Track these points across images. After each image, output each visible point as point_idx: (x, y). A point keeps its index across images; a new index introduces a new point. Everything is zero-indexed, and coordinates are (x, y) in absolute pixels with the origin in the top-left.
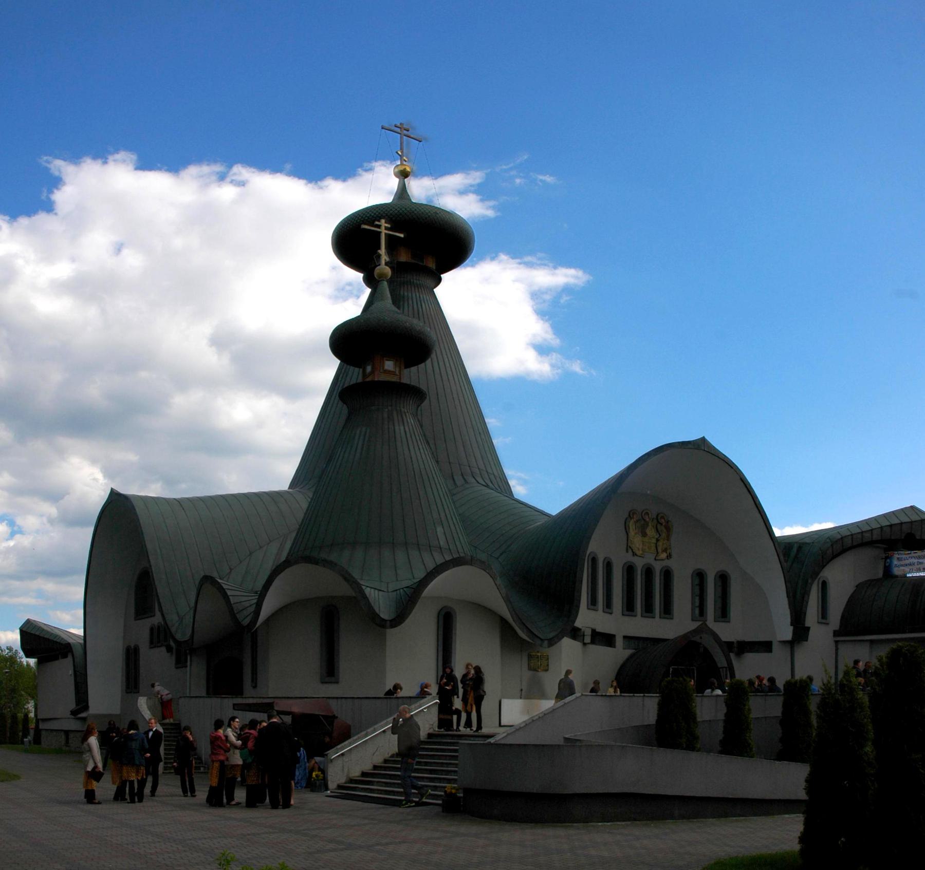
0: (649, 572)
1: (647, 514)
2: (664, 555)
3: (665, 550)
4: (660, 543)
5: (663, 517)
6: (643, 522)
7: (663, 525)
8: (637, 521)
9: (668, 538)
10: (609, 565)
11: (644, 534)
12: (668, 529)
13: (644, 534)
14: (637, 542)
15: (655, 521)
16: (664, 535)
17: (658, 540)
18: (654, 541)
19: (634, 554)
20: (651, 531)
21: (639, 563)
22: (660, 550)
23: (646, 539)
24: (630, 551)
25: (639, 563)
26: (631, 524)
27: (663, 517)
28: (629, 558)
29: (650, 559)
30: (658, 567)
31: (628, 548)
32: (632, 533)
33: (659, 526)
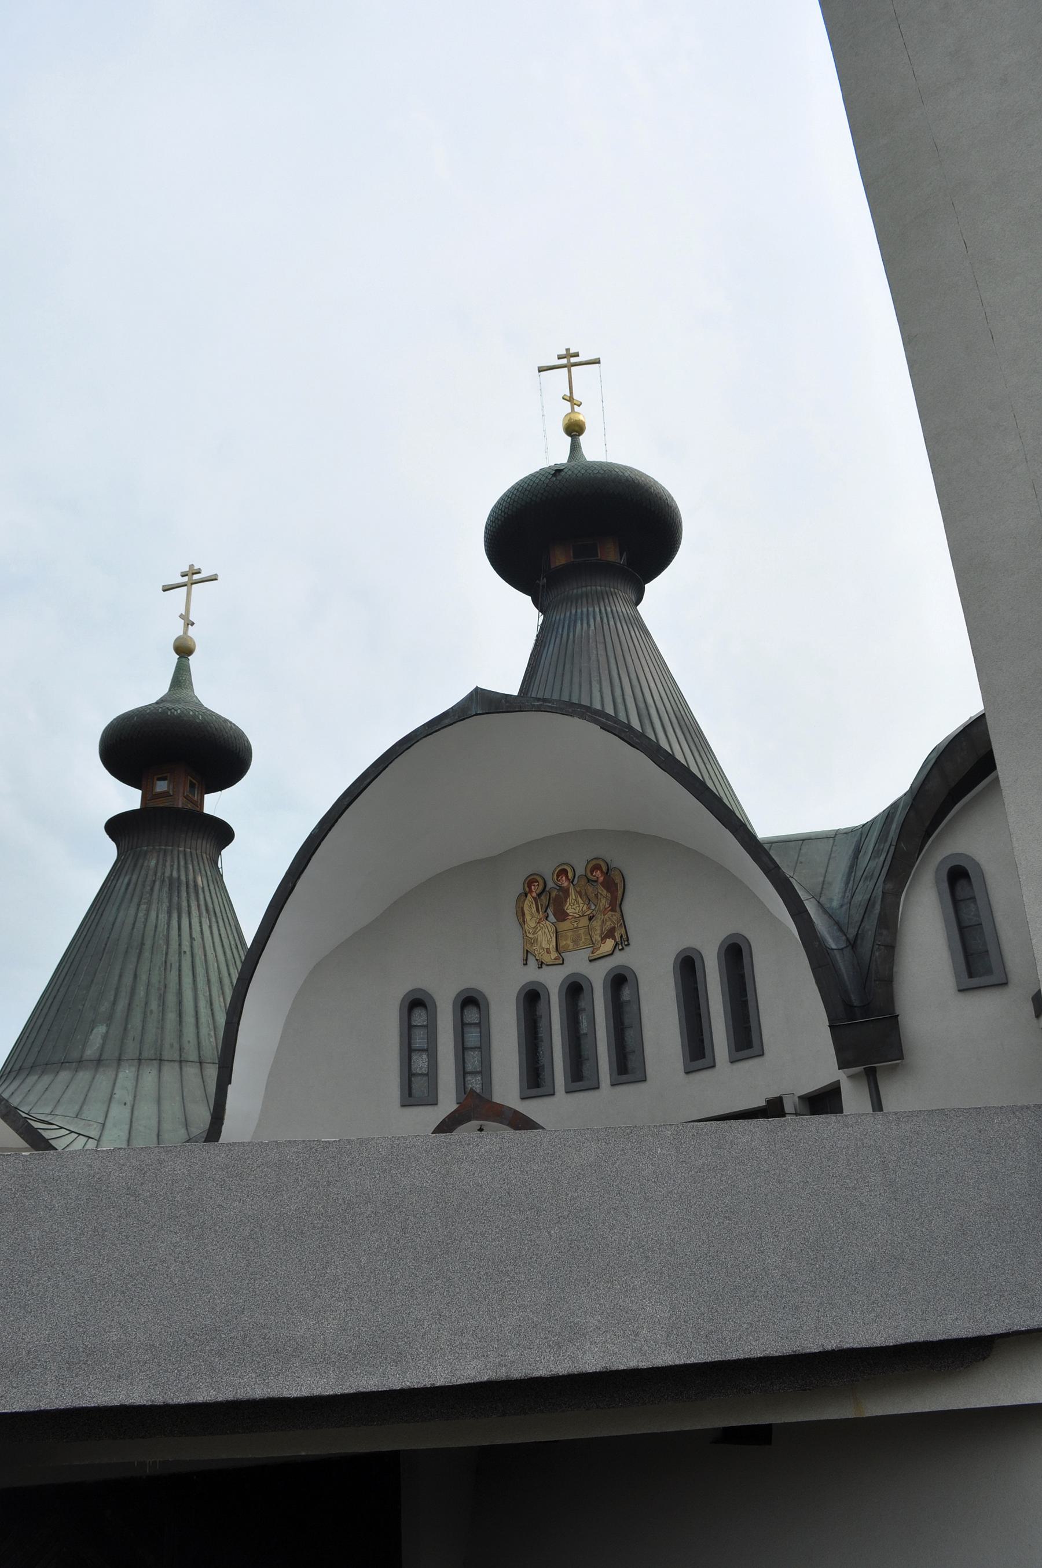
0: (575, 990)
1: (564, 872)
2: (609, 944)
3: (610, 934)
4: (596, 924)
5: (597, 867)
7: (608, 883)
8: (539, 895)
9: (616, 904)
11: (561, 916)
15: (583, 881)
16: (604, 903)
20: (574, 906)
23: (564, 926)
25: (553, 980)
27: (597, 867)
28: (532, 974)
29: (577, 963)
32: (531, 923)
33: (590, 889)
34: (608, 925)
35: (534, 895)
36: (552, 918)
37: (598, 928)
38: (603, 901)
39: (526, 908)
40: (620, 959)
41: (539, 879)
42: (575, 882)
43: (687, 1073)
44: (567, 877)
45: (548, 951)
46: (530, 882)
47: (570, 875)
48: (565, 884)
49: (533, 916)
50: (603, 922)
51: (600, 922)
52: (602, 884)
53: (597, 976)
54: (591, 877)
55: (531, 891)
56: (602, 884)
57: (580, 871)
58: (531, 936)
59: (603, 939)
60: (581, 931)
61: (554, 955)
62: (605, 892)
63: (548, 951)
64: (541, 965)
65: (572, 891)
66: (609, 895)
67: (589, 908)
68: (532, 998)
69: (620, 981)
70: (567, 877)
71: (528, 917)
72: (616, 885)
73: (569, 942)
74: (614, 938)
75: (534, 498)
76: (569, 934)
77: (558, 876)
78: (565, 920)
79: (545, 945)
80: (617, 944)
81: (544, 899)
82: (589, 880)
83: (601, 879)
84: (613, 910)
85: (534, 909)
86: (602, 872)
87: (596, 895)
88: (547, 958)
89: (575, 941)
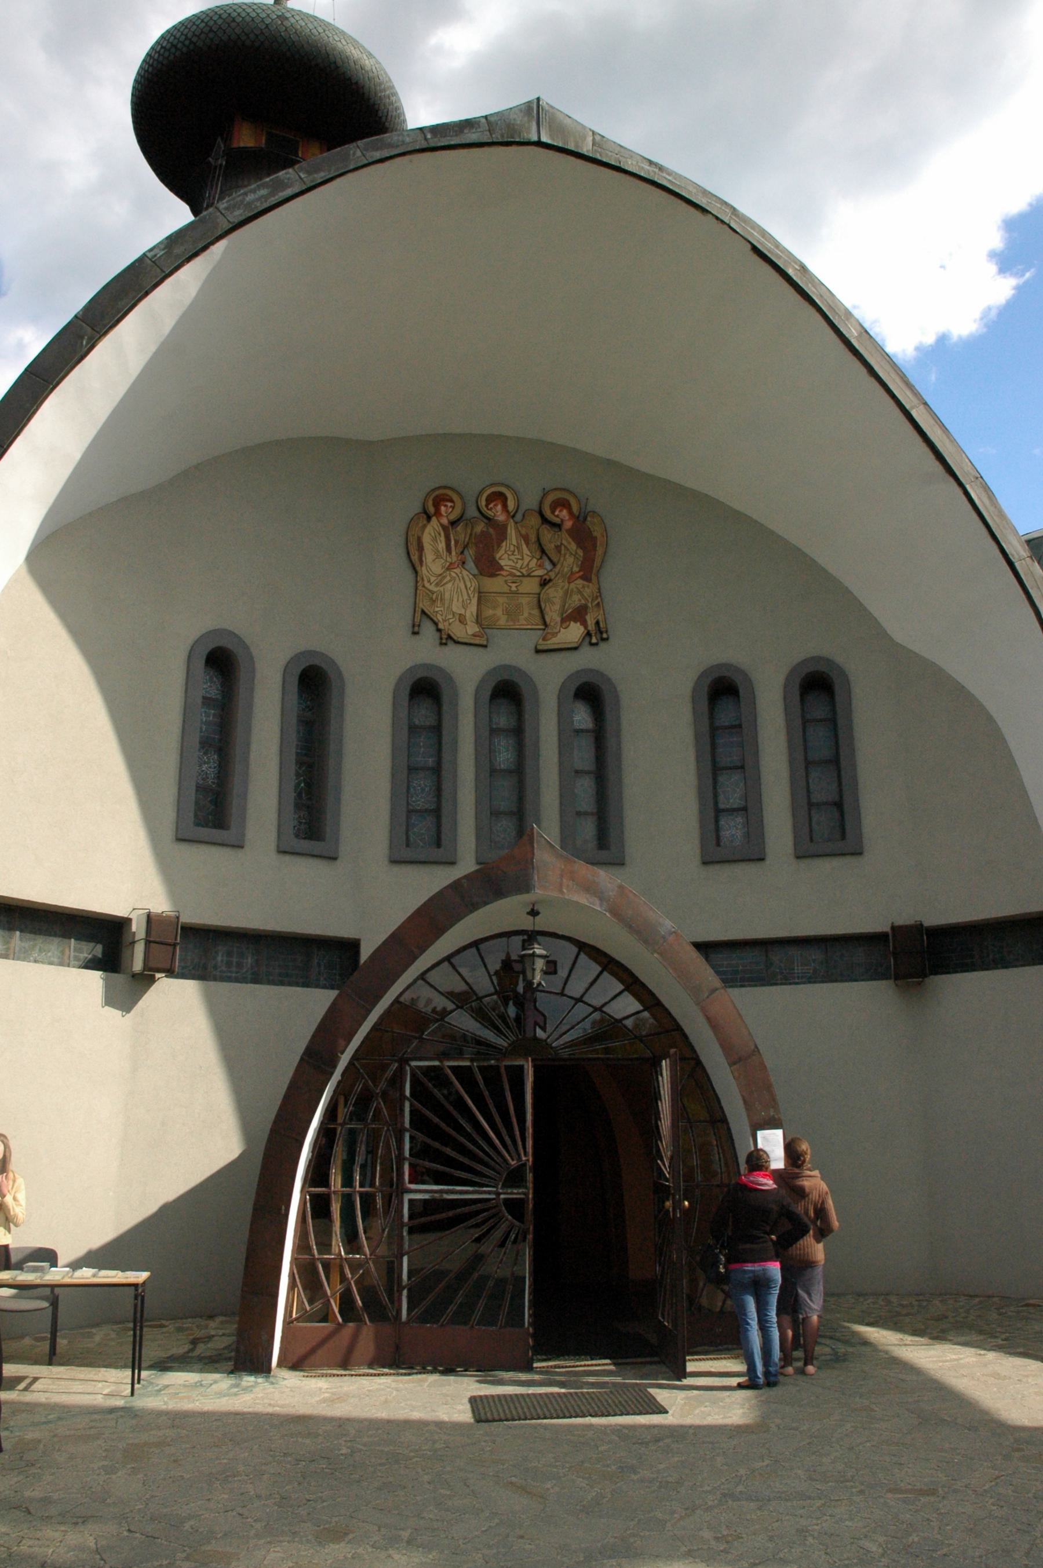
0: (507, 692)
2: (574, 632)
3: (578, 615)
4: (554, 594)
5: (564, 504)
6: (480, 527)
8: (453, 523)
9: (588, 570)
10: (314, 685)
11: (488, 567)
12: (586, 535)
13: (488, 567)
14: (457, 595)
15: (535, 521)
16: (570, 562)
17: (544, 583)
18: (531, 586)
19: (446, 639)
20: (514, 555)
21: (467, 672)
22: (553, 615)
24: (428, 629)
25: (467, 672)
26: (432, 535)
28: (425, 651)
29: (512, 650)
30: (549, 679)
31: (421, 619)
33: (548, 536)
34: (576, 600)
35: (445, 521)
36: (470, 564)
37: (558, 601)
38: (570, 560)
39: (426, 539)
40: (588, 659)
41: (455, 497)
42: (519, 517)
43: (705, 863)
44: (505, 506)
45: (462, 620)
46: (438, 499)
47: (511, 505)
48: (501, 517)
49: (438, 556)
50: (567, 593)
51: (561, 593)
52: (570, 532)
53: (549, 679)
54: (548, 513)
55: (438, 513)
56: (570, 532)
57: (530, 501)
58: (432, 588)
59: (567, 619)
60: (524, 600)
61: (472, 628)
62: (573, 546)
63: (462, 620)
64: (446, 639)
65: (511, 532)
66: (580, 553)
67: (541, 566)
68: (425, 690)
69: (590, 693)
70: (505, 506)
71: (429, 556)
72: (594, 539)
73: (499, 612)
74: (584, 623)
75: (244, 38)
76: (501, 600)
77: (489, 501)
78: (493, 575)
79: (457, 607)
80: (589, 634)
81: (460, 533)
82: (545, 520)
83: (568, 524)
84: (586, 578)
85: (442, 545)
86: (571, 513)
87: (558, 548)
88: (458, 631)
89: (512, 613)
